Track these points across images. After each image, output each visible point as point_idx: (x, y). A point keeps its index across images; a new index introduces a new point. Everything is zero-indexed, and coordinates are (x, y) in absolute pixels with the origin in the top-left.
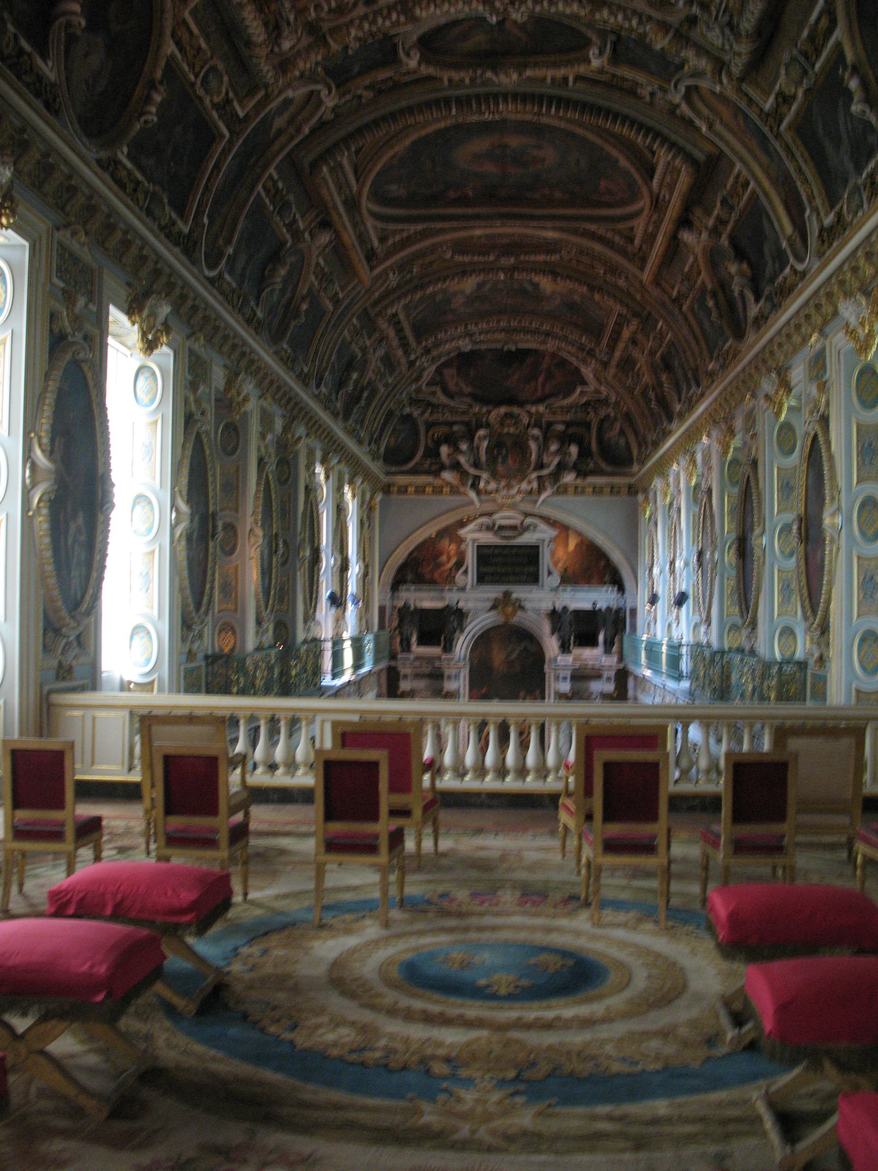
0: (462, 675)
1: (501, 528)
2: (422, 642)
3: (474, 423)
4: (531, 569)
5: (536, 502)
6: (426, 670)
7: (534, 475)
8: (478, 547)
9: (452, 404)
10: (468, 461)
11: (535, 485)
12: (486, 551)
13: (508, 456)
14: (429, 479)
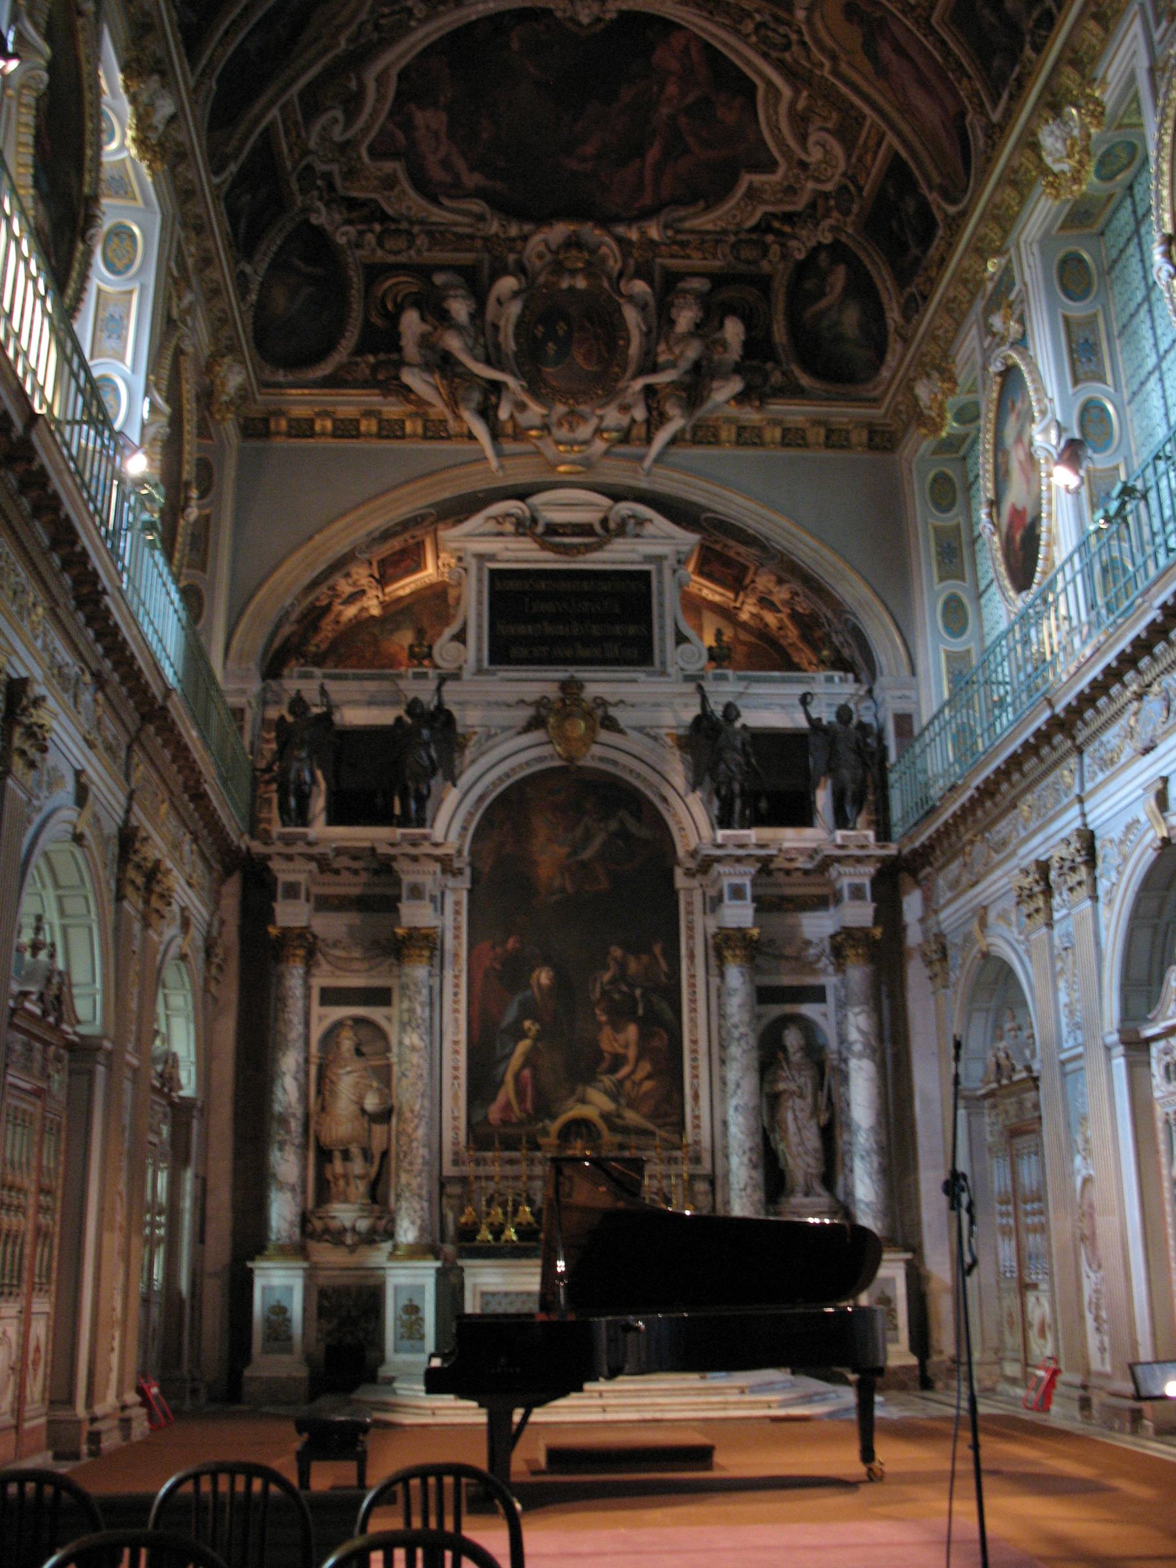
0: (449, 901)
1: (553, 529)
2: (336, 817)
3: (486, 266)
4: (632, 630)
5: (641, 458)
6: (350, 886)
7: (638, 384)
8: (494, 573)
9: (438, 215)
10: (471, 351)
11: (639, 414)
12: (512, 585)
13: (569, 344)
14: (373, 399)
